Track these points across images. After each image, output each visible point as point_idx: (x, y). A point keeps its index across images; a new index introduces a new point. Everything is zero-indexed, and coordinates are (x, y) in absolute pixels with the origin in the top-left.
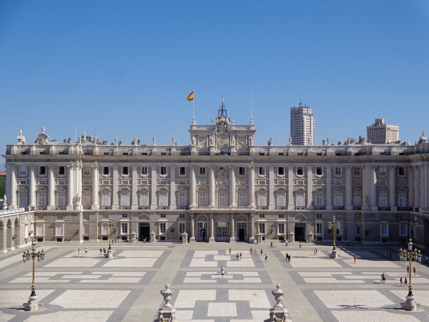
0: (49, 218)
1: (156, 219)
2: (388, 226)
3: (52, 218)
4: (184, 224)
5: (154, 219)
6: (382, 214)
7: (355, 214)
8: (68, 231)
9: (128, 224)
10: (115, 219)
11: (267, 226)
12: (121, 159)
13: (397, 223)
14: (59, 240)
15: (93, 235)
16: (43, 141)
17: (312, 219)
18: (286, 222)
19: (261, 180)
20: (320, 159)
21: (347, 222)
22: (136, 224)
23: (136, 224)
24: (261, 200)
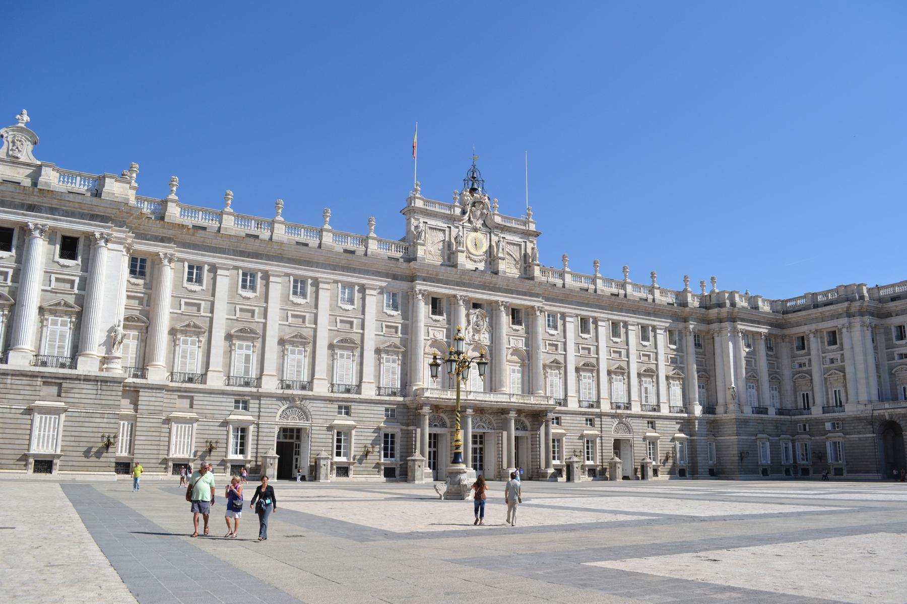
0: (12, 391)
1: (328, 417)
2: (768, 444)
3: (22, 392)
4: (393, 436)
5: (322, 417)
6: (759, 421)
7: (707, 422)
8: (77, 439)
9: (252, 428)
10: (212, 412)
11: (566, 444)
12: (242, 247)
13: (777, 438)
14: (44, 465)
15: (146, 456)
16: (19, 151)
17: (641, 431)
18: (597, 436)
19: (551, 342)
20: (647, 309)
21: (695, 438)
22: (272, 430)
23: (272, 430)
24: (552, 385)
